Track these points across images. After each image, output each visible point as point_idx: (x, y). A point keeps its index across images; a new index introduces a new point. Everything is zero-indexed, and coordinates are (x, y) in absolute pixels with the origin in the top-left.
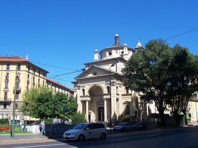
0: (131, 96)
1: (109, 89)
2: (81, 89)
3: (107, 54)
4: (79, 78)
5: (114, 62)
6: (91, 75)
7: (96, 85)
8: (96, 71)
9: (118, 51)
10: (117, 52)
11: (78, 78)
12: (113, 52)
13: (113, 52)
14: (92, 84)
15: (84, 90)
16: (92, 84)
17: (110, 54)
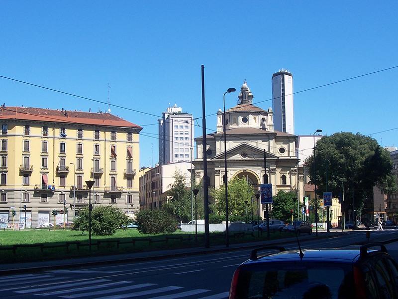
0: (290, 188)
1: (266, 177)
2: (222, 175)
3: (240, 118)
4: (217, 160)
5: (264, 139)
6: (238, 157)
7: (247, 171)
8: (247, 151)
9: (257, 117)
10: (255, 118)
11: (218, 158)
12: (251, 117)
13: (251, 117)
14: (239, 170)
15: (225, 178)
16: (239, 170)
17: (245, 120)
